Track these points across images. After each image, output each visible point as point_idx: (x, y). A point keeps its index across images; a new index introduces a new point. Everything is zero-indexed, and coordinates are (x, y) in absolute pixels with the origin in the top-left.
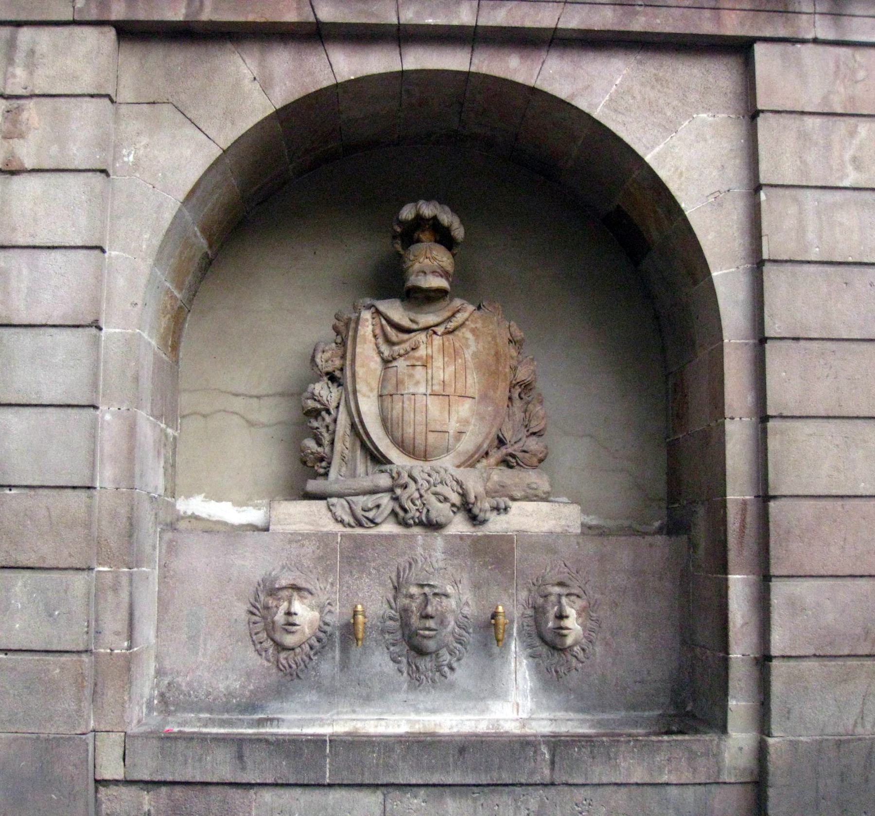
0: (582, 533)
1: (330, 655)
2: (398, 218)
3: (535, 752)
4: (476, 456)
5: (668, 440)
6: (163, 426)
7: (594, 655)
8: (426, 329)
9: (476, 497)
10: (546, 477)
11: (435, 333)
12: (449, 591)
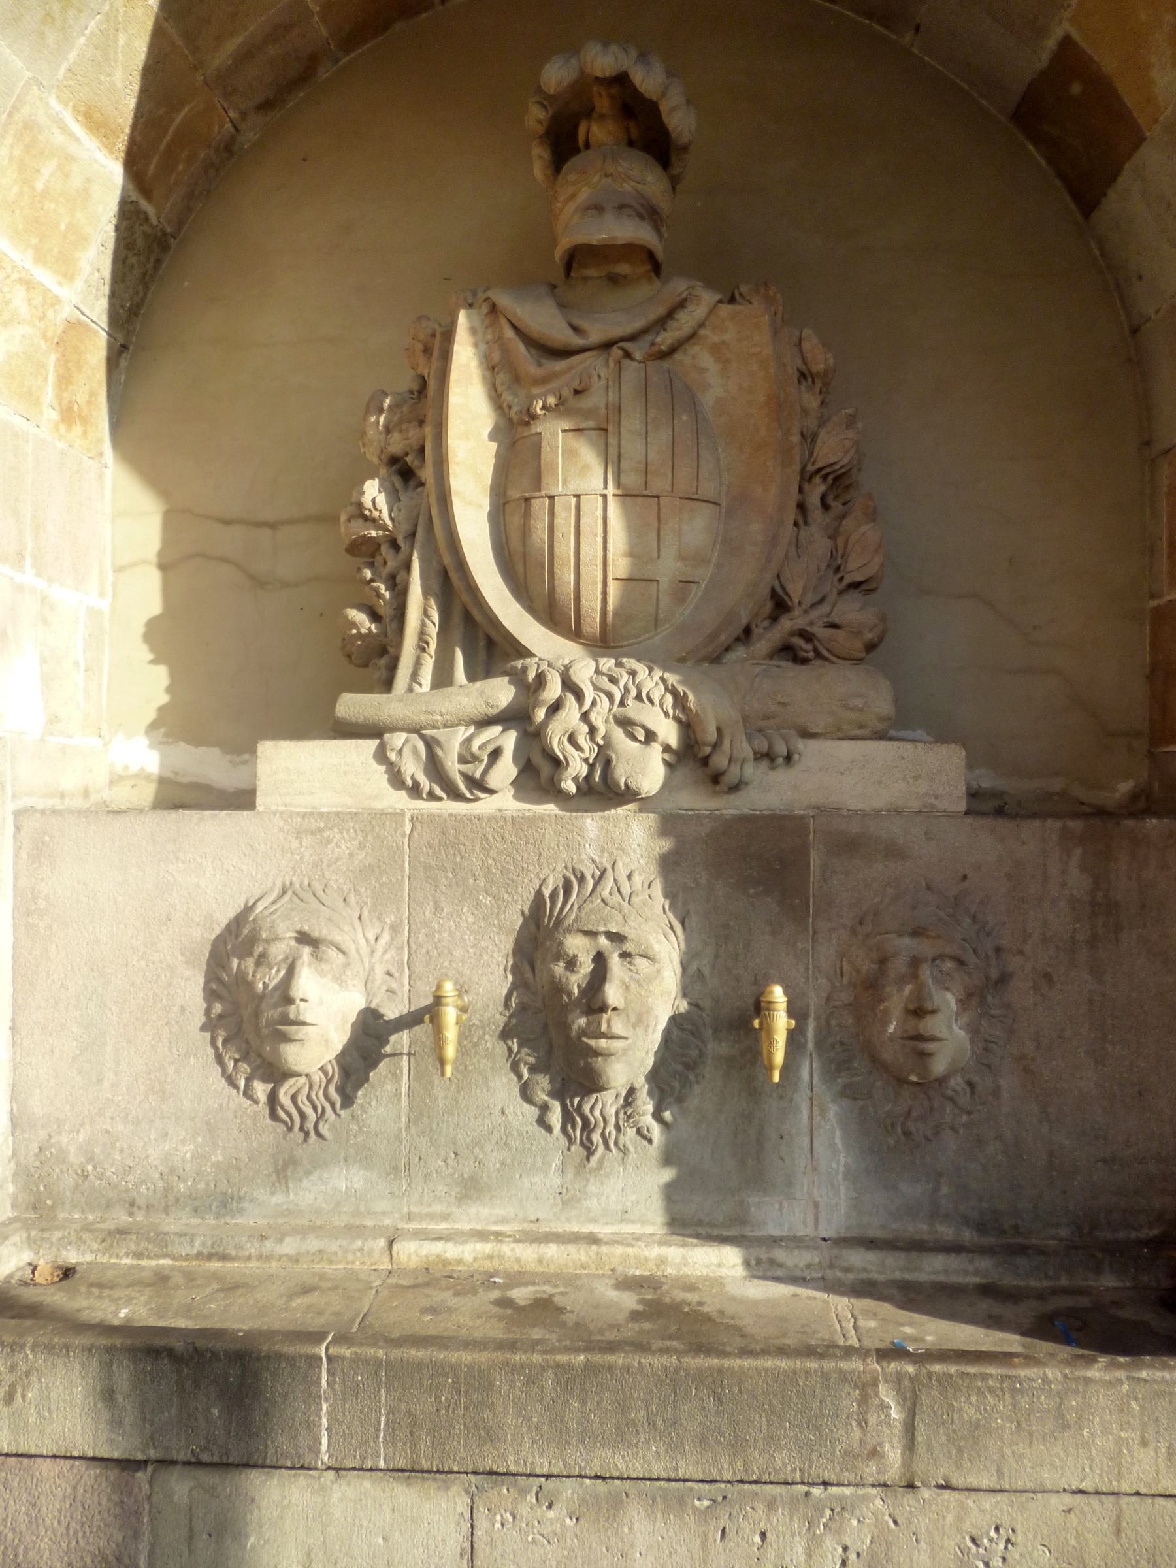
0: (967, 813)
1: (389, 1087)
2: (539, 90)
3: (864, 1401)
4: (722, 638)
5: (1154, 603)
6: (28, 577)
7: (996, 1092)
8: (607, 346)
9: (719, 730)
10: (885, 685)
11: (628, 355)
12: (656, 947)
